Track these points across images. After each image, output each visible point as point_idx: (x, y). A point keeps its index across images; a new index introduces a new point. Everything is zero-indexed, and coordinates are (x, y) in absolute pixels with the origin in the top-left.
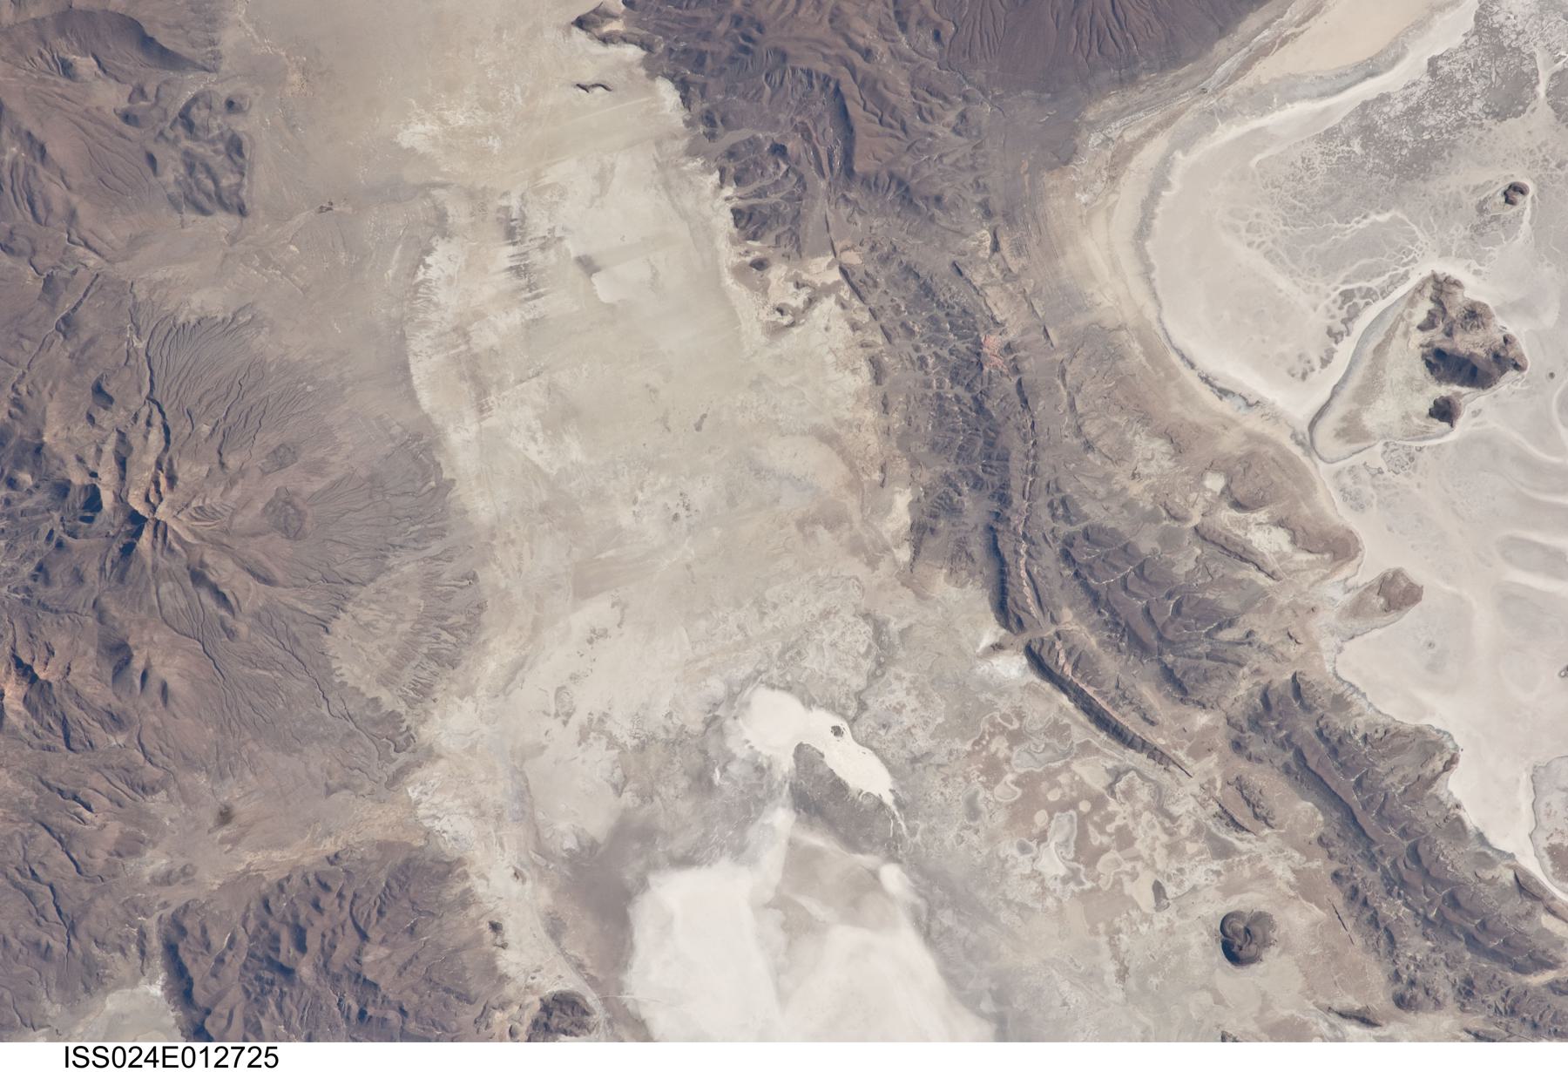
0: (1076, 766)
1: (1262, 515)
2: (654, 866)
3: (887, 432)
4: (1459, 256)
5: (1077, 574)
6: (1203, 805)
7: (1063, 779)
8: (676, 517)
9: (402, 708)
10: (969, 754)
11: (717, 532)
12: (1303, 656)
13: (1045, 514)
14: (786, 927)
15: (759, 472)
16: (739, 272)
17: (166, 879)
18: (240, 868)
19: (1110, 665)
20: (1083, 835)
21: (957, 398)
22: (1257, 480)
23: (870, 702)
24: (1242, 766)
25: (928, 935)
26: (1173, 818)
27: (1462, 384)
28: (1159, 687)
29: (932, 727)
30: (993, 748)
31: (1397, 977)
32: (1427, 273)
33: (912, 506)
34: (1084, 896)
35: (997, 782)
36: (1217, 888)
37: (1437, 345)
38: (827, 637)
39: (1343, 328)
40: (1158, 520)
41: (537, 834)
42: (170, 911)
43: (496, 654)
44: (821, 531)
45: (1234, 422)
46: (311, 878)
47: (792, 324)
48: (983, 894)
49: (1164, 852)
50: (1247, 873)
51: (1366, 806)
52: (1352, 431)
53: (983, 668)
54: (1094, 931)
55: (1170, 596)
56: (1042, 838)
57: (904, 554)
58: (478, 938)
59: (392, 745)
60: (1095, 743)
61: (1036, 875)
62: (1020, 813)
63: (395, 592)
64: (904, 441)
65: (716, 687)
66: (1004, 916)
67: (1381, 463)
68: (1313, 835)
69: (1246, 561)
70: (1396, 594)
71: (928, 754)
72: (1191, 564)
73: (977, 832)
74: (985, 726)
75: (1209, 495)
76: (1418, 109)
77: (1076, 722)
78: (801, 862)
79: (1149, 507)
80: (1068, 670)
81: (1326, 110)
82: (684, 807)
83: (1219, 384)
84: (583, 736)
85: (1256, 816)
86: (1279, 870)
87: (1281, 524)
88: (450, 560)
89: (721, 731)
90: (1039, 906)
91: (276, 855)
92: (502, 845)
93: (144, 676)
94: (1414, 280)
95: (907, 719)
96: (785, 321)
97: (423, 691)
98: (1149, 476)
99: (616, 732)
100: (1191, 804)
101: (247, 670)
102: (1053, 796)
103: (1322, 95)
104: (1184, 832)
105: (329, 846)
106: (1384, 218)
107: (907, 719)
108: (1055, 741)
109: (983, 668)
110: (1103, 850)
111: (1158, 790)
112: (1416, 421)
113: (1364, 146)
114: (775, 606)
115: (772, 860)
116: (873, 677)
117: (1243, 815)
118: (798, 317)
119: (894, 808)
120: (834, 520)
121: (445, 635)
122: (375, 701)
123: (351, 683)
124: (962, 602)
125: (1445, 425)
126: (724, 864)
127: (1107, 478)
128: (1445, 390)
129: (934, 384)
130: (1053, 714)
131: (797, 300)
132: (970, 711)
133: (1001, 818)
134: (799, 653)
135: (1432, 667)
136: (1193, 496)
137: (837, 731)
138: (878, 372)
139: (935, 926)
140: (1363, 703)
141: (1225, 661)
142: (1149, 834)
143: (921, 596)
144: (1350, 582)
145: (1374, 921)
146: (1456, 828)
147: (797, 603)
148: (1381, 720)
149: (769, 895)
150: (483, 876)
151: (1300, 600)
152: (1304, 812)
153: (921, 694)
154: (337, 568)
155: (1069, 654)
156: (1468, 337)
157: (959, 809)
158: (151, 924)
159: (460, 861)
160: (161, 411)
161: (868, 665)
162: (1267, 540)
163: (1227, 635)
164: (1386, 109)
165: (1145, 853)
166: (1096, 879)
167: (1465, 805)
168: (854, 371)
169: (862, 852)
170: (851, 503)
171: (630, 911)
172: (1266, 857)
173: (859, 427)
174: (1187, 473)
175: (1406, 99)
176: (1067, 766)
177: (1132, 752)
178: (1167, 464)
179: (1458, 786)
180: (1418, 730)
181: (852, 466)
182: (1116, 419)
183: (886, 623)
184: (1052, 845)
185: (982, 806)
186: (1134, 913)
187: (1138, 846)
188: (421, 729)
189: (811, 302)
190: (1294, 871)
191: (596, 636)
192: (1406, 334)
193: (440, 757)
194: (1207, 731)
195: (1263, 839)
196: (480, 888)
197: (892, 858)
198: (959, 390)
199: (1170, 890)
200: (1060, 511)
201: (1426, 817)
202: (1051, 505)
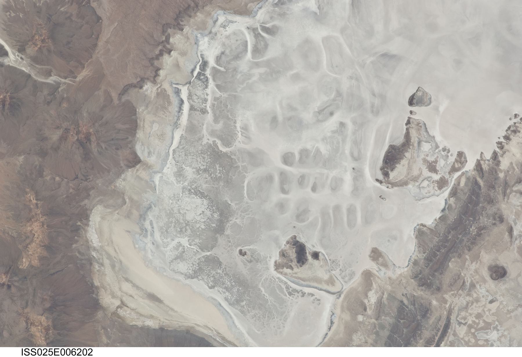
1: (366, 301)
4: (267, 264)
6: (461, 295)
12: (405, 277)
22: (355, 304)
24: (445, 287)
27: (306, 253)
28: (429, 318)
32: (275, 272)
36: (485, 284)
37: (296, 263)
39: (300, 292)
45: (340, 317)
49: (479, 303)
50: (477, 277)
51: (445, 247)
52: (331, 281)
67: (338, 270)
69: (381, 303)
70: (376, 255)
72: (388, 318)
75: (365, 319)
76: (226, 288)
81: (235, 315)
83: (330, 325)
85: (459, 278)
86: (473, 268)
94: (279, 275)
103: (231, 317)
104: (471, 299)
106: (262, 289)
110: (484, 321)
111: (460, 310)
112: (322, 263)
113: (243, 301)
125: (320, 254)
128: (309, 257)
135: (395, 239)
140: (413, 256)
141: (414, 301)
142: (475, 309)
144: (378, 270)
145: (479, 235)
146: (442, 219)
148: (417, 249)
151: (388, 283)
152: (452, 265)
156: (291, 255)
162: (373, 298)
163: (406, 302)
164: (229, 298)
165: (481, 309)
167: (434, 218)
172: (471, 272)
175: (224, 293)
177: (451, 321)
179: (430, 221)
180: (416, 238)
187: (480, 311)
190: (472, 263)
192: (296, 273)
194: (437, 300)
195: (465, 275)
199: (490, 298)
201: (442, 229)
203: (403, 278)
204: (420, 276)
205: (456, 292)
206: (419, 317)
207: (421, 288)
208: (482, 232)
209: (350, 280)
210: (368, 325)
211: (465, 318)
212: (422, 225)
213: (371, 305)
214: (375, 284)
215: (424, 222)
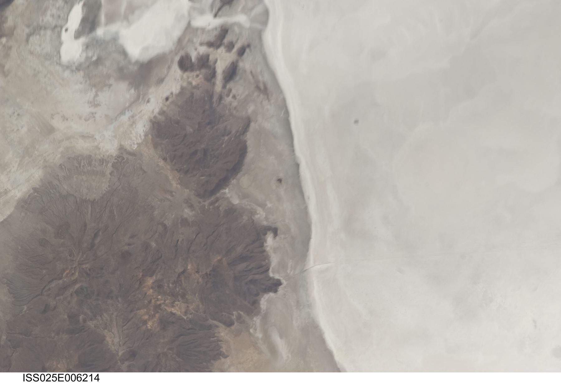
2: (130, 62)
9: (110, 165)
17: (191, 207)
18: (179, 186)
41: (134, 102)
42: (201, 200)
43: (82, 146)
46: (173, 163)
58: (172, 102)
59: (123, 160)
63: (74, 187)
65: (67, 74)
82: (108, 63)
88: (58, 176)
89: (80, 65)
91: (171, 178)
92: (141, 111)
93: (129, 245)
97: (102, 161)
99: (92, 96)
101: (116, 217)
105: (162, 163)
121: (82, 164)
122: (111, 174)
123: (108, 184)
150: (153, 112)
154: (74, 208)
158: (206, 203)
159: (151, 121)
160: (44, 288)
188: (114, 155)
191: (65, 119)
193: (121, 145)
196: (157, 111)
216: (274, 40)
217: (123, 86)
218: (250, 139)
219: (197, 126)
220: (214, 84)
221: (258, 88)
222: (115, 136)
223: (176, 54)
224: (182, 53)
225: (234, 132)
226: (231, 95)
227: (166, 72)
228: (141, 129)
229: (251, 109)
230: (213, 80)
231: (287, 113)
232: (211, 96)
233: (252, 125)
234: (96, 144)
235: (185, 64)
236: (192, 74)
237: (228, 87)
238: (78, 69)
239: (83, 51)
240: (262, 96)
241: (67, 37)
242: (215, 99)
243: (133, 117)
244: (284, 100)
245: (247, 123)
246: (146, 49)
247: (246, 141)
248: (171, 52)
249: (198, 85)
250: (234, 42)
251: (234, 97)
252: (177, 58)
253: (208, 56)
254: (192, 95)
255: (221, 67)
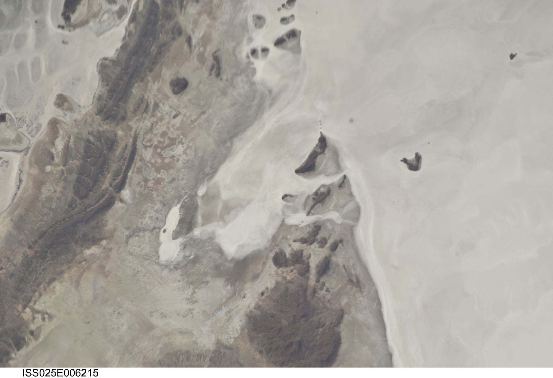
0: (148, 159)
1: (53, 150)
2: (226, 260)
3: (69, 268)
5: (91, 191)
6: (145, 119)
7: (153, 161)
8: (119, 313)
10: (156, 191)
11: (118, 299)
13: (76, 210)
14: (228, 213)
15: (95, 297)
16: (36, 338)
19: (114, 167)
20: (168, 146)
21: (51, 254)
22: (43, 156)
23: (152, 227)
24: (129, 114)
25: (215, 170)
26: (152, 124)
29: (153, 205)
30: (152, 185)
31: (173, 39)
33: (88, 248)
34: (185, 136)
35: (161, 178)
38: (138, 250)
40: (66, 178)
41: (230, 298)
44: (107, 268)
47: (47, 313)
48: (196, 164)
50: (160, 96)
53: (129, 201)
54: (194, 127)
55: (86, 161)
56: (173, 157)
57: (104, 242)
58: (267, 297)
60: (139, 158)
61: (185, 153)
62: (167, 167)
64: (70, 262)
65: (165, 272)
66: (200, 154)
68: (142, 84)
70: (62, 101)
71: (161, 202)
72: (75, 161)
73: (178, 176)
74: (146, 191)
75: (53, 168)
77: (135, 167)
78: (207, 219)
79: (63, 182)
80: (120, 177)
82: (205, 261)
84: (196, 302)
85: (142, 102)
86: (156, 88)
87: (53, 144)
89: (178, 264)
90: (193, 147)
92: (237, 306)
95: (153, 214)
96: (47, 316)
98: (53, 187)
99: (190, 293)
100: (146, 122)
102: (159, 161)
104: (155, 119)
107: (153, 214)
108: (143, 170)
109: (129, 201)
110: (170, 138)
111: (146, 133)
114: (134, 270)
115: (210, 228)
116: (144, 230)
117: (143, 106)
118: (43, 313)
119: (181, 203)
120: (102, 267)
124: (113, 219)
126: (217, 240)
127: (59, 199)
129: (49, 263)
130: (135, 174)
131: (39, 316)
132: (144, 197)
133: (172, 171)
134: (146, 255)
136: (55, 172)
137: (164, 231)
138: (52, 280)
139: (211, 171)
141: (100, 136)
142: (160, 128)
143: (115, 230)
144: (63, 115)
147: (131, 264)
148: (100, 84)
149: (221, 223)
150: (249, 306)
152: (136, 91)
153: (144, 213)
155: (116, 179)
157: (174, 185)
159: (247, 315)
161: (141, 234)
162: (60, 144)
163: (92, 139)
165: (166, 126)
166: (179, 135)
167: (115, 49)
168: (54, 288)
169: (197, 204)
170: (94, 266)
171: (242, 259)
173: (70, 277)
174: (48, 178)
176: (149, 162)
177: (138, 147)
178: (48, 184)
179: (111, 53)
180: (100, 72)
181: (84, 272)
182: (40, 206)
183: (127, 236)
184: (174, 153)
185: (170, 179)
186: (185, 119)
189: (38, 312)
190: (154, 83)
191: (163, 316)
193: (218, 340)
194: (123, 130)
195: (148, 97)
196: (253, 305)
197: (196, 194)
198: (48, 255)
199: (174, 113)
200: (74, 206)
202: (73, 210)
203: (88, 117)
204: (105, 110)
205: (140, 116)
206: (105, 152)
207: (106, 121)
208: (163, 49)
209: (37, 133)
210: (56, 174)
211: (150, 140)
212: (105, 59)
213: (58, 153)
214: (62, 130)
215: (106, 56)
216: (366, 235)
217: (220, 283)
218: (344, 331)
219: (292, 319)
220: (308, 278)
221: (351, 281)
222: (212, 332)
223: (271, 251)
224: (276, 250)
225: (328, 324)
226: (325, 289)
227: (261, 268)
228: (237, 323)
229: (344, 301)
230: (307, 275)
231: (379, 304)
232: (305, 290)
233: (346, 316)
234: (194, 339)
235: (280, 260)
236: (287, 269)
237: (321, 280)
238: (176, 268)
239: (181, 250)
240: (355, 289)
241: (164, 238)
242: (309, 293)
243: (229, 312)
244: (376, 292)
245: (341, 315)
246: (242, 246)
247: (339, 333)
248: (266, 248)
249: (293, 279)
250: (327, 237)
251: (328, 290)
252: (272, 255)
253: (301, 252)
254: (287, 289)
255: (314, 262)
